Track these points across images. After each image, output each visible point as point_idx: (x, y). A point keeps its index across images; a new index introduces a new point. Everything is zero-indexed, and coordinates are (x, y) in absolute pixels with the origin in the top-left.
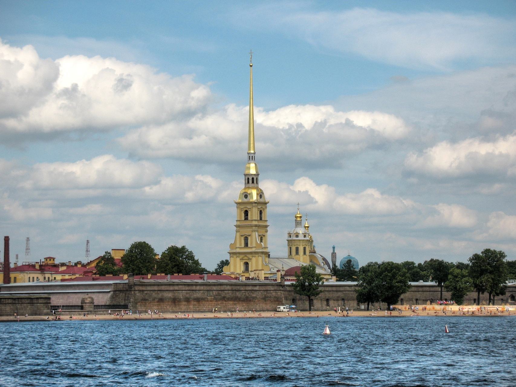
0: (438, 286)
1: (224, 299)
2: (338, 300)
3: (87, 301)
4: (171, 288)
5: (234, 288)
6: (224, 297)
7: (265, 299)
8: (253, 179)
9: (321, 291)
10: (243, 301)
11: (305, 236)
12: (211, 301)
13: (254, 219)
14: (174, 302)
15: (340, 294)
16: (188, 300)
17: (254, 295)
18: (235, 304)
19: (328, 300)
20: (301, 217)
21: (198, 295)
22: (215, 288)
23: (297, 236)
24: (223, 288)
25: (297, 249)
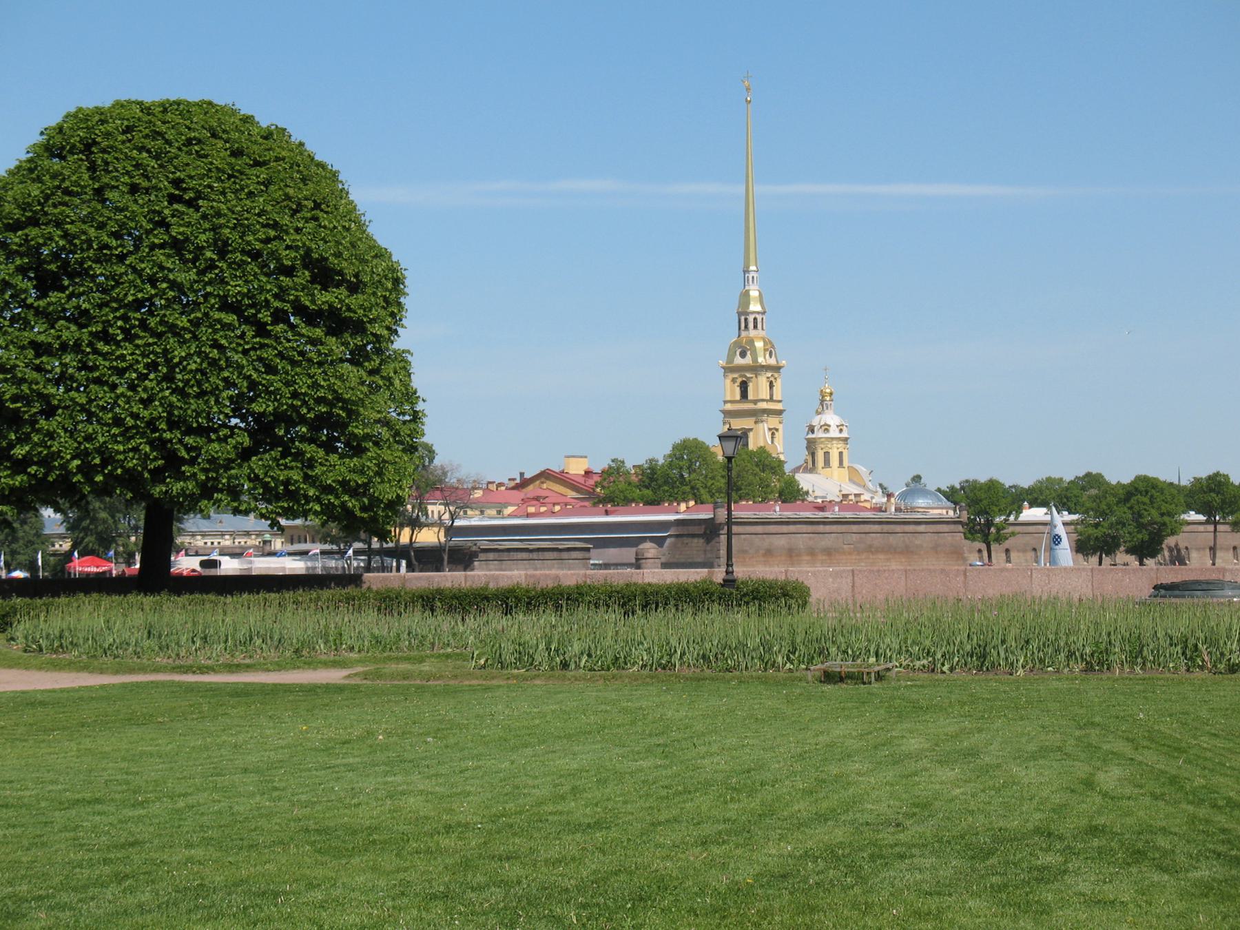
0: (1207, 522)
1: (870, 549)
2: (1024, 551)
3: (649, 555)
4: (785, 529)
5: (886, 528)
6: (870, 546)
7: (935, 549)
8: (755, 319)
9: (1013, 534)
10: (901, 553)
11: (841, 431)
12: (850, 554)
13: (761, 397)
14: (791, 556)
15: (1027, 538)
16: (812, 552)
17: (917, 542)
18: (888, 560)
19: (1007, 551)
20: (831, 394)
21: (827, 541)
22: (854, 528)
23: (827, 430)
24: (867, 528)
25: (827, 454)
